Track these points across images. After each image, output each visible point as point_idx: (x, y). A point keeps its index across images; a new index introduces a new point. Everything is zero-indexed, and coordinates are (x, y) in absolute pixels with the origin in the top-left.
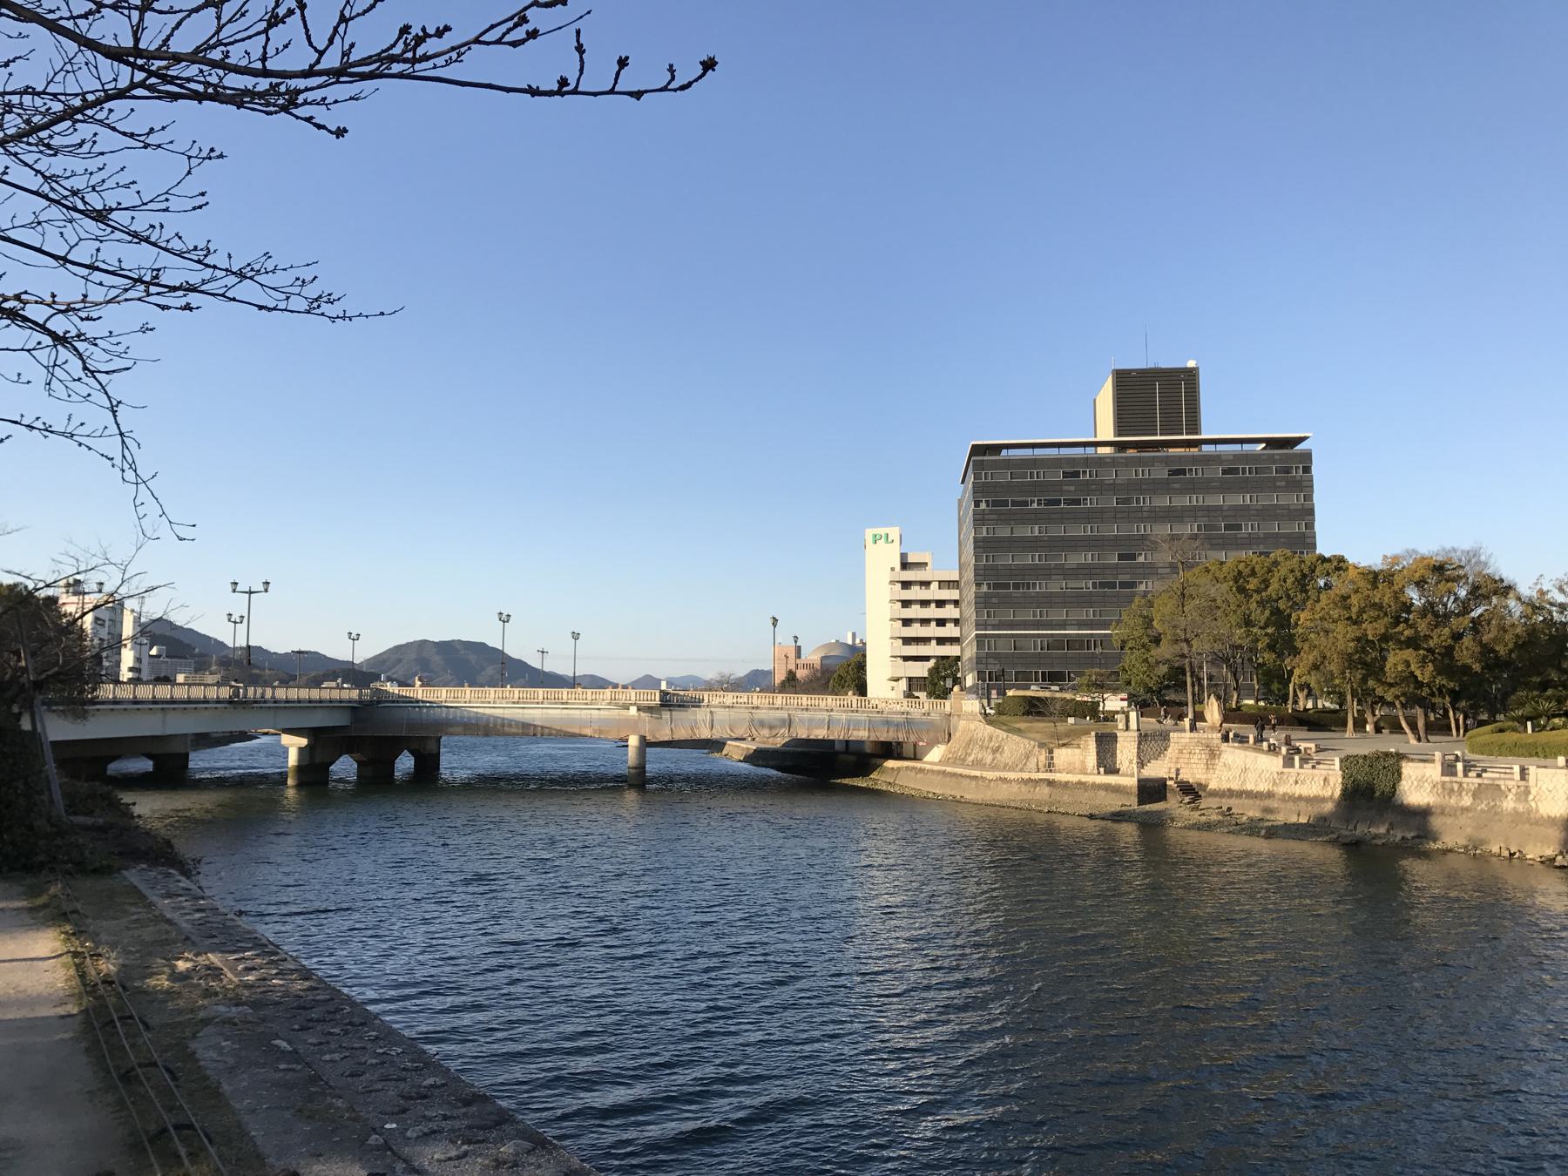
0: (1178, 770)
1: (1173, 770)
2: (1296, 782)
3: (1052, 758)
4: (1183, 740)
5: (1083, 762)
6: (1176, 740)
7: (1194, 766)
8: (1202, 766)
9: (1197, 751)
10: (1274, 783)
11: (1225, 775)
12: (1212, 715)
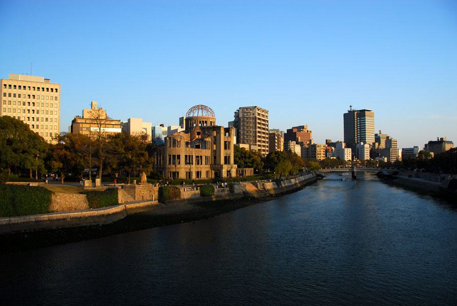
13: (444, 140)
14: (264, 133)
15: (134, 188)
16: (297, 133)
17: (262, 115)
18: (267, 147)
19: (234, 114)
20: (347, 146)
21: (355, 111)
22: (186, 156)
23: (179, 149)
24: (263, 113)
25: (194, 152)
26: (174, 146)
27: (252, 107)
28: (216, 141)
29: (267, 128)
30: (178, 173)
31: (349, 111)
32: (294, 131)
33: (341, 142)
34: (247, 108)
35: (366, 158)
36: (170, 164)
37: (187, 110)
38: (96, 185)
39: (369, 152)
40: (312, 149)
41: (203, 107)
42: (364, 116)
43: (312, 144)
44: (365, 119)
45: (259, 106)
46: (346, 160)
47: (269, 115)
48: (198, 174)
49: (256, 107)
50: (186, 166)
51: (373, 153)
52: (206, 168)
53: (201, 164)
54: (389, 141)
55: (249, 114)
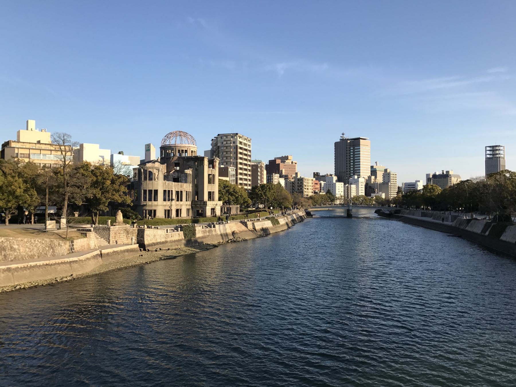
0: (116, 242)
1: (115, 241)
2: (172, 237)
3: (73, 245)
4: (116, 229)
5: (88, 244)
6: (113, 229)
7: (122, 238)
8: (125, 238)
9: (122, 233)
10: (166, 238)
11: (149, 239)
12: (120, 218)
13: (451, 173)
14: (246, 165)
16: (281, 165)
17: (244, 143)
18: (250, 180)
19: (211, 142)
20: (339, 180)
21: (348, 139)
22: (165, 191)
24: (245, 142)
25: (174, 187)
26: (151, 179)
27: (233, 134)
28: (198, 175)
29: (249, 158)
30: (155, 211)
32: (277, 163)
33: (331, 175)
34: (226, 136)
36: (145, 200)
37: (163, 136)
38: (62, 227)
39: (364, 187)
40: (298, 183)
41: (181, 134)
42: (359, 145)
43: (299, 177)
46: (337, 196)
48: (178, 212)
49: (237, 134)
50: (165, 203)
51: (369, 188)
52: (187, 205)
53: (181, 200)
54: (387, 175)
55: (229, 142)
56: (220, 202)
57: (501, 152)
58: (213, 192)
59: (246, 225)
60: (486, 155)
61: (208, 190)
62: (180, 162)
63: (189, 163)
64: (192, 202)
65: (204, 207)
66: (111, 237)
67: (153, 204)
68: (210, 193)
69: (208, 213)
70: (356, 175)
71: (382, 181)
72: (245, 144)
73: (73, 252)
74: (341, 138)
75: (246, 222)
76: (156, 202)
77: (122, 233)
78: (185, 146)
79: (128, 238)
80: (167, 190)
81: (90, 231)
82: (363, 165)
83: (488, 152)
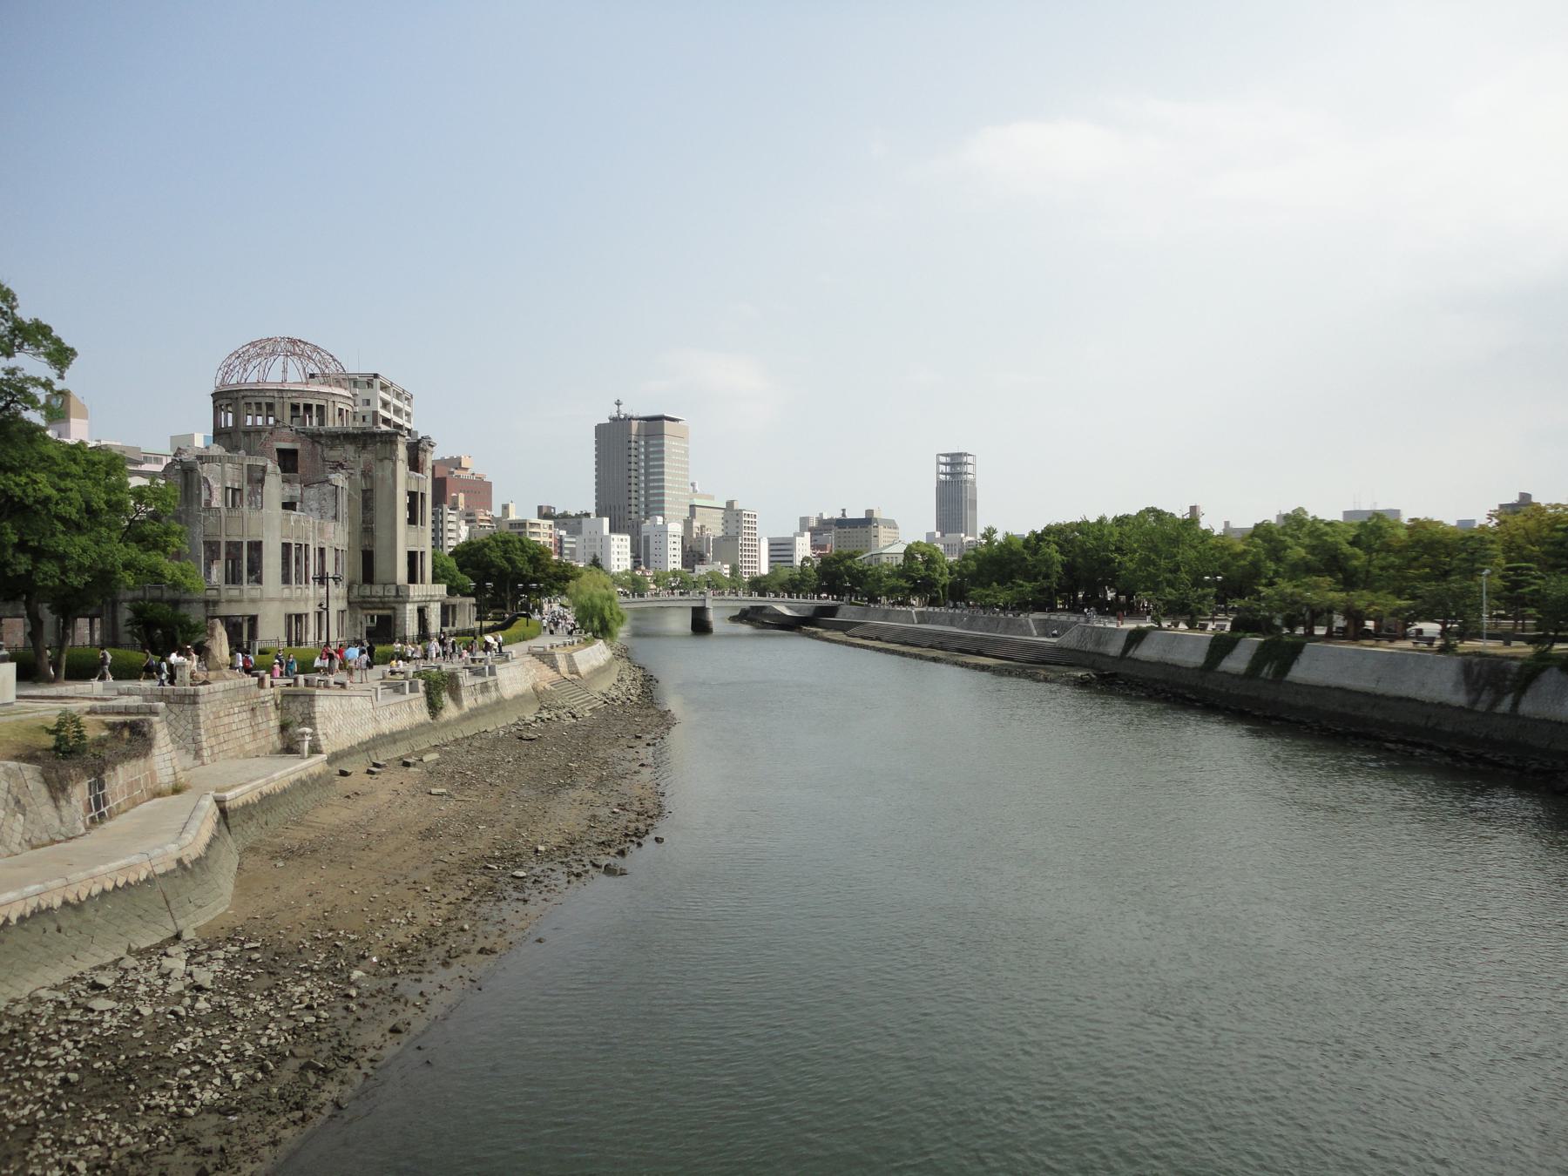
7: (238, 734)
8: (249, 731)
12: (221, 650)
13: (876, 515)
15: (193, 699)
17: (395, 406)
20: (614, 529)
21: (631, 419)
22: (286, 547)
23: (255, 515)
27: (362, 375)
30: (253, 620)
31: (614, 419)
33: (587, 515)
35: (671, 567)
44: (663, 445)
45: (387, 375)
47: (415, 408)
49: (376, 376)
50: (286, 592)
52: (337, 598)
54: (732, 514)
56: (437, 585)
57: (970, 469)
58: (422, 553)
59: (554, 667)
60: (938, 473)
61: (407, 545)
62: (297, 446)
63: (336, 454)
64: (350, 588)
65: (393, 605)
66: (202, 732)
67: (245, 597)
68: (412, 556)
69: (412, 628)
70: (659, 515)
71: (720, 533)
72: (397, 411)
73: (102, 815)
74: (615, 415)
75: (553, 654)
76: (257, 586)
77: (236, 710)
78: (318, 392)
79: (256, 728)
80: (293, 541)
81: (156, 714)
82: (670, 488)
83: (942, 468)
